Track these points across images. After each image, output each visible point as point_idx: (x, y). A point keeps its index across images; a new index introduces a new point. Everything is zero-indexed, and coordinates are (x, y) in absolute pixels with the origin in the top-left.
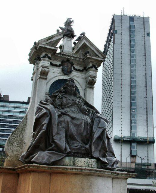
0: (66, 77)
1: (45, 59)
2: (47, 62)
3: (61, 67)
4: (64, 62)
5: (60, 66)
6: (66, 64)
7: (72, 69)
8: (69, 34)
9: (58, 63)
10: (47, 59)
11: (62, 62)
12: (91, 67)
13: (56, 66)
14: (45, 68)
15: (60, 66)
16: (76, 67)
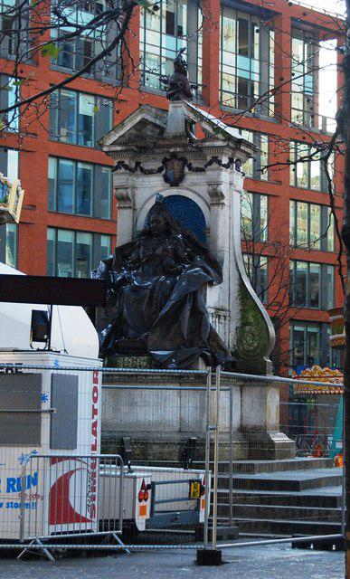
0: (174, 191)
1: (119, 171)
2: (122, 177)
3: (164, 172)
4: (169, 160)
5: (160, 170)
6: (170, 164)
7: (186, 170)
8: (174, 93)
9: (156, 165)
10: (123, 170)
11: (165, 161)
12: (210, 163)
13: (150, 172)
14: (120, 191)
15: (160, 170)
16: (195, 165)
